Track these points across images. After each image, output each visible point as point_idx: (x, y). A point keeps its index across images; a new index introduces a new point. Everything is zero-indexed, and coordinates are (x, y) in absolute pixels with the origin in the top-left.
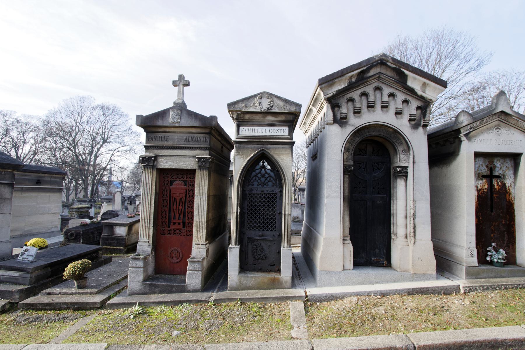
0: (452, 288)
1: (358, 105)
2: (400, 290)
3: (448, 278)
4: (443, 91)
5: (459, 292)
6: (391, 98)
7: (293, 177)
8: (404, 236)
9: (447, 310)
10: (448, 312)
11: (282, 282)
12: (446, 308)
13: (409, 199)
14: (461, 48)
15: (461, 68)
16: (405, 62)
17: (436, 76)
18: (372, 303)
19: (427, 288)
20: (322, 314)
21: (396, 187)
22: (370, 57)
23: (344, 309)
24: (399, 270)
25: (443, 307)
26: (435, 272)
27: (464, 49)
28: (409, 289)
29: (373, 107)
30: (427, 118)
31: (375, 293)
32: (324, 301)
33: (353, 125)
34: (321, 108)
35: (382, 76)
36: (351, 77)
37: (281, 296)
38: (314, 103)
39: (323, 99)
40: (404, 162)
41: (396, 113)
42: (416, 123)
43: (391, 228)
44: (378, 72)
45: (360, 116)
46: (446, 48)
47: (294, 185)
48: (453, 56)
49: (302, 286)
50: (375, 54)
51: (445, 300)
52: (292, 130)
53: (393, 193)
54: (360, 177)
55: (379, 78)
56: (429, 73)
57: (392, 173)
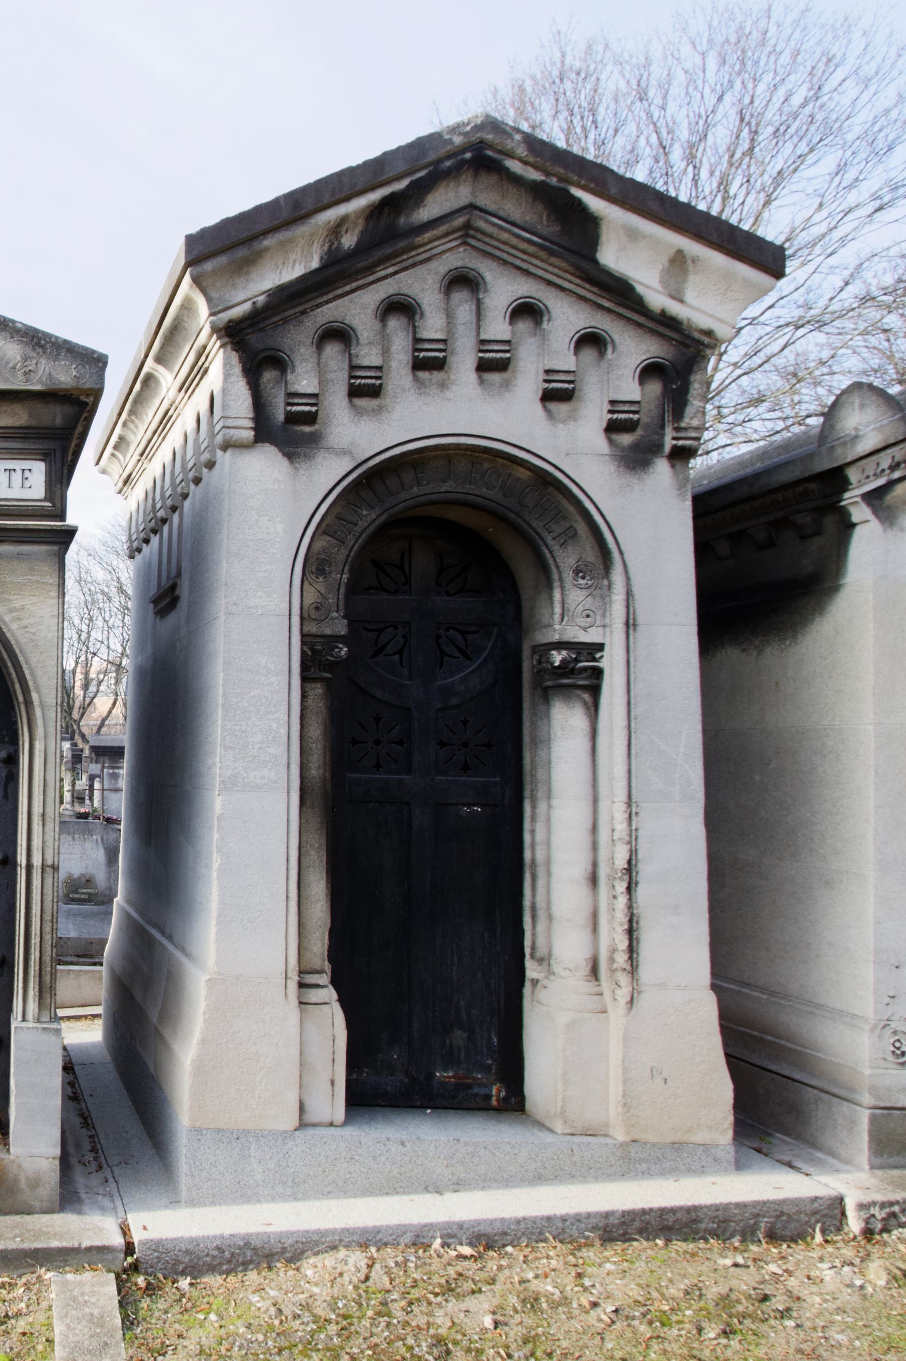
0: (809, 1208)
1: (369, 356)
2: (564, 1219)
3: (790, 1165)
4: (765, 292)
5: (839, 1229)
6: (524, 325)
7: (67, 692)
8: (586, 969)
9: (784, 1314)
10: (790, 1323)
11: (16, 1180)
12: (779, 1302)
13: (610, 799)
14: (851, 90)
15: (850, 187)
16: (590, 156)
17: (734, 221)
18: (436, 1279)
19: (689, 1210)
20: (204, 1331)
21: (548, 741)
22: (425, 131)
23: (306, 1307)
24: (559, 1127)
25: (765, 1298)
26: (730, 1134)
27: (865, 97)
28: (607, 1215)
29: (438, 365)
30: (690, 419)
31: (451, 1234)
32: (212, 1269)
33: (345, 452)
34: (198, 371)
35: (481, 224)
36: (337, 229)
37: (12, 1245)
38: (163, 347)
39: (207, 330)
40: (582, 621)
41: (549, 397)
42: (639, 441)
43: (522, 932)
44: (463, 202)
45: (381, 409)
46: (781, 93)
47: (70, 731)
48: (812, 127)
49: (106, 1202)
50: (450, 118)
51: (773, 1268)
52: (61, 475)
53: (534, 767)
54: (378, 693)
55: (467, 233)
56: (702, 206)
57: (526, 675)
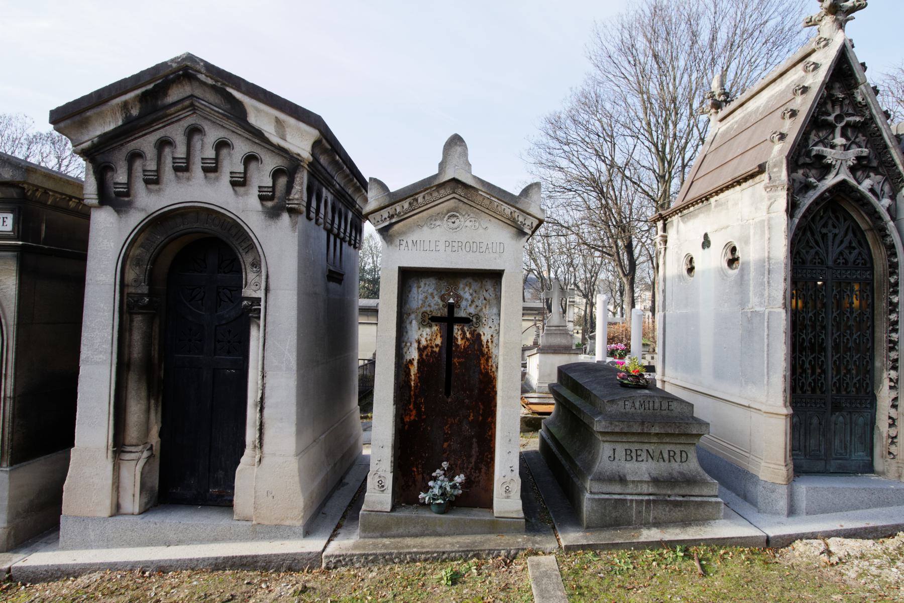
33: (143, 210)
35: (197, 104)
44: (188, 94)
45: (160, 190)
55: (193, 108)
